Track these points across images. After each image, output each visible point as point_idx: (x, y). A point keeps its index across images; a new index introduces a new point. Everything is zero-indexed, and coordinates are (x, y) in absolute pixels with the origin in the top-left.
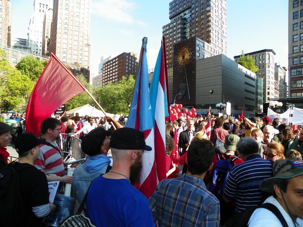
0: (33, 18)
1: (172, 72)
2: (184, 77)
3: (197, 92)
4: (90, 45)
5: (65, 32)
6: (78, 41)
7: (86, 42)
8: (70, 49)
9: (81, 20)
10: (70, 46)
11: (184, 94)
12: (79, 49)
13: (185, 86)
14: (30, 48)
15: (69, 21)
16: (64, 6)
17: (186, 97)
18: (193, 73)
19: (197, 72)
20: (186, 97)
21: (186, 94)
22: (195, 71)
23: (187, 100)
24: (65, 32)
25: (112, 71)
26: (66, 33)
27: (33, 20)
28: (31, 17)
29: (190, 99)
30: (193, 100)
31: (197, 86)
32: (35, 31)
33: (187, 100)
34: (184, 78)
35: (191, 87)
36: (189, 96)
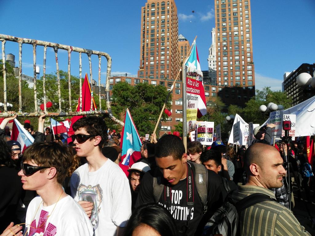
0: (211, 50)
4: (253, 63)
5: (225, 55)
6: (239, 61)
7: (249, 60)
8: (231, 71)
9: (241, 38)
10: (231, 68)
12: (241, 69)
14: (210, 79)
15: (228, 42)
16: (221, 29)
24: (225, 54)
25: (292, 89)
26: (226, 55)
27: (211, 52)
28: (210, 49)
32: (214, 62)
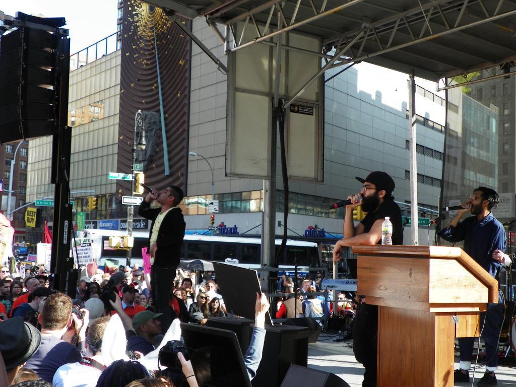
1: (119, 68)
2: (152, 85)
3: (193, 143)
11: (148, 154)
13: (155, 122)
17: (157, 167)
18: (180, 65)
19: (195, 61)
20: (157, 167)
21: (156, 153)
22: (188, 58)
23: (159, 177)
29: (167, 172)
30: (178, 178)
31: (193, 120)
33: (159, 177)
34: (152, 90)
35: (173, 122)
36: (166, 163)
